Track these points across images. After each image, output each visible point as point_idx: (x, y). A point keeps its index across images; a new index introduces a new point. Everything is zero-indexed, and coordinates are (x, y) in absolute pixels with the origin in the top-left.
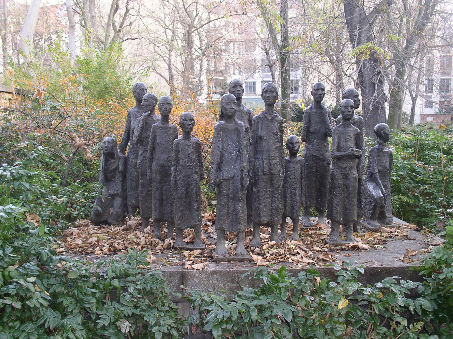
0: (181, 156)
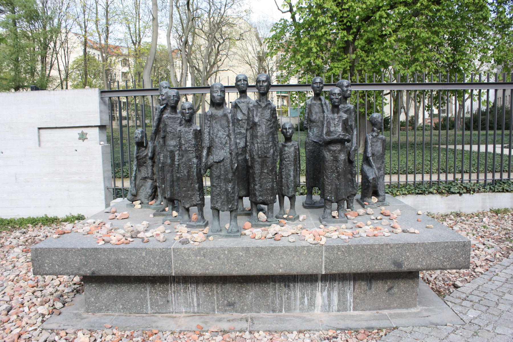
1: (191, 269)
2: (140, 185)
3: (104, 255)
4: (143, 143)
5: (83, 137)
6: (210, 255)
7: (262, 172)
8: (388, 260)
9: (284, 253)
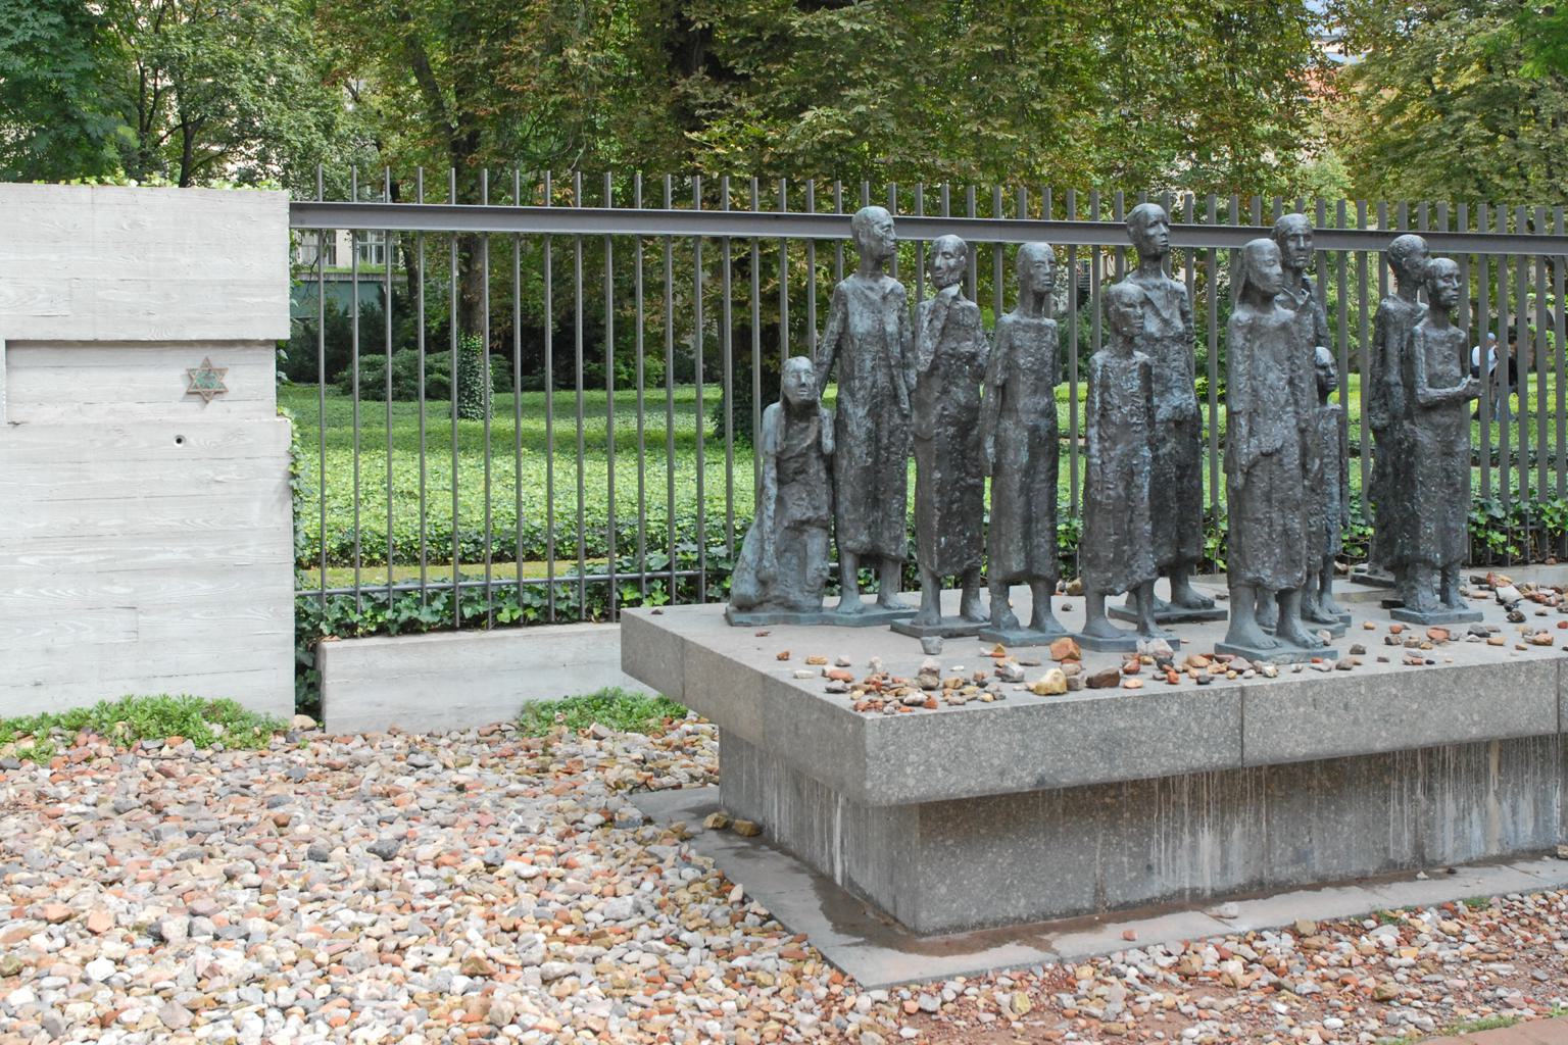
1: (1283, 744)
3: (1074, 723)
5: (205, 388)
9: (1481, 683)
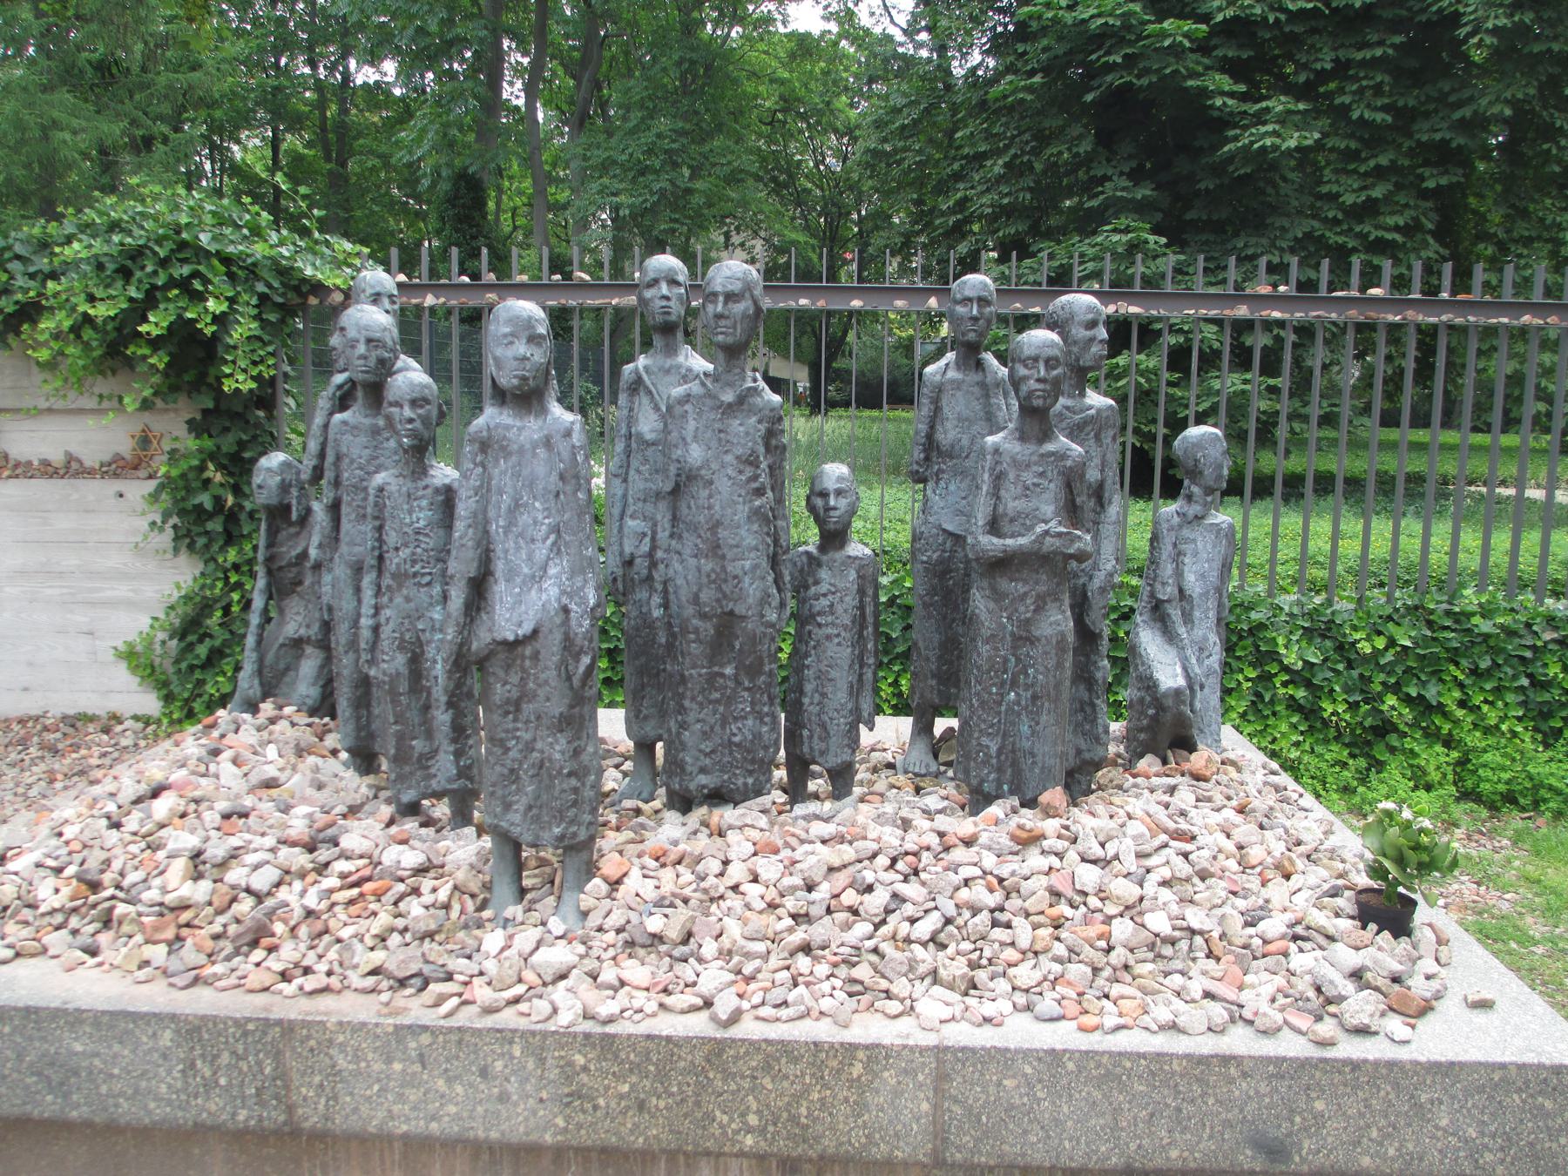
0: (392, 538)
1: (364, 1109)
2: (282, 666)
4: (288, 508)
6: (448, 1060)
7: (712, 678)
8: (1228, 1124)
9: (767, 1067)
